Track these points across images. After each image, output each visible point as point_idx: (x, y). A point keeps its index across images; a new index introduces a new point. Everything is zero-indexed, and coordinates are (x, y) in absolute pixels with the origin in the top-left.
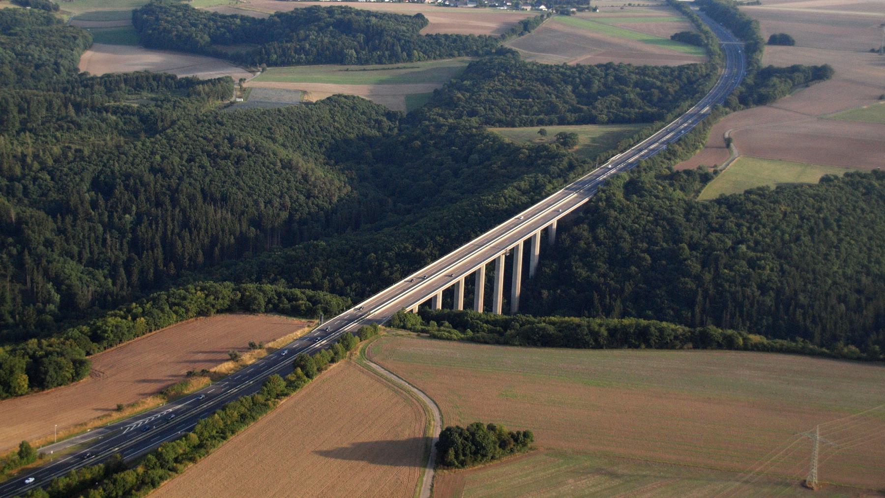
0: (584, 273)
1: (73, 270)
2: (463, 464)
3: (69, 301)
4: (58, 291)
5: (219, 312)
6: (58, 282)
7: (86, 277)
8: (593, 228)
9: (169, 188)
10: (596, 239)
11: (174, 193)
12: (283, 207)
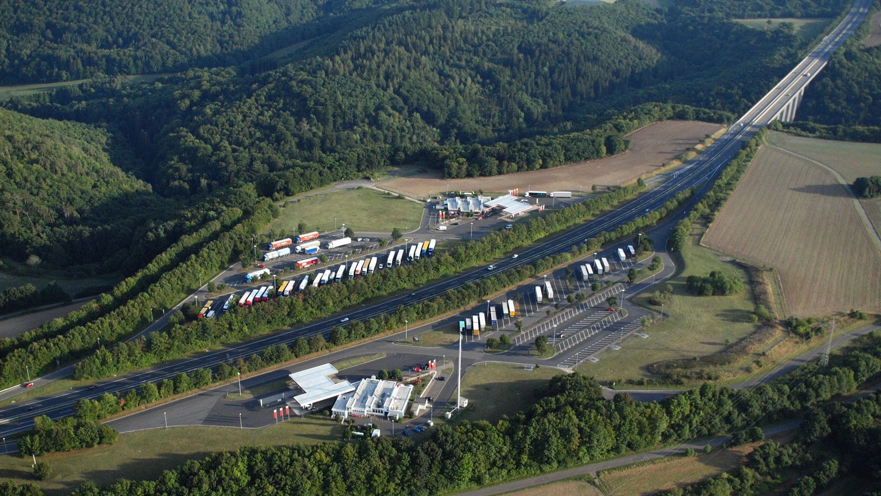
0: (833, 106)
1: (527, 99)
2: (872, 196)
3: (529, 118)
4: (522, 110)
5: (668, 119)
6: (521, 106)
7: (534, 104)
8: (833, 80)
9: (563, 51)
10: (836, 86)
11: (568, 54)
12: (628, 64)
